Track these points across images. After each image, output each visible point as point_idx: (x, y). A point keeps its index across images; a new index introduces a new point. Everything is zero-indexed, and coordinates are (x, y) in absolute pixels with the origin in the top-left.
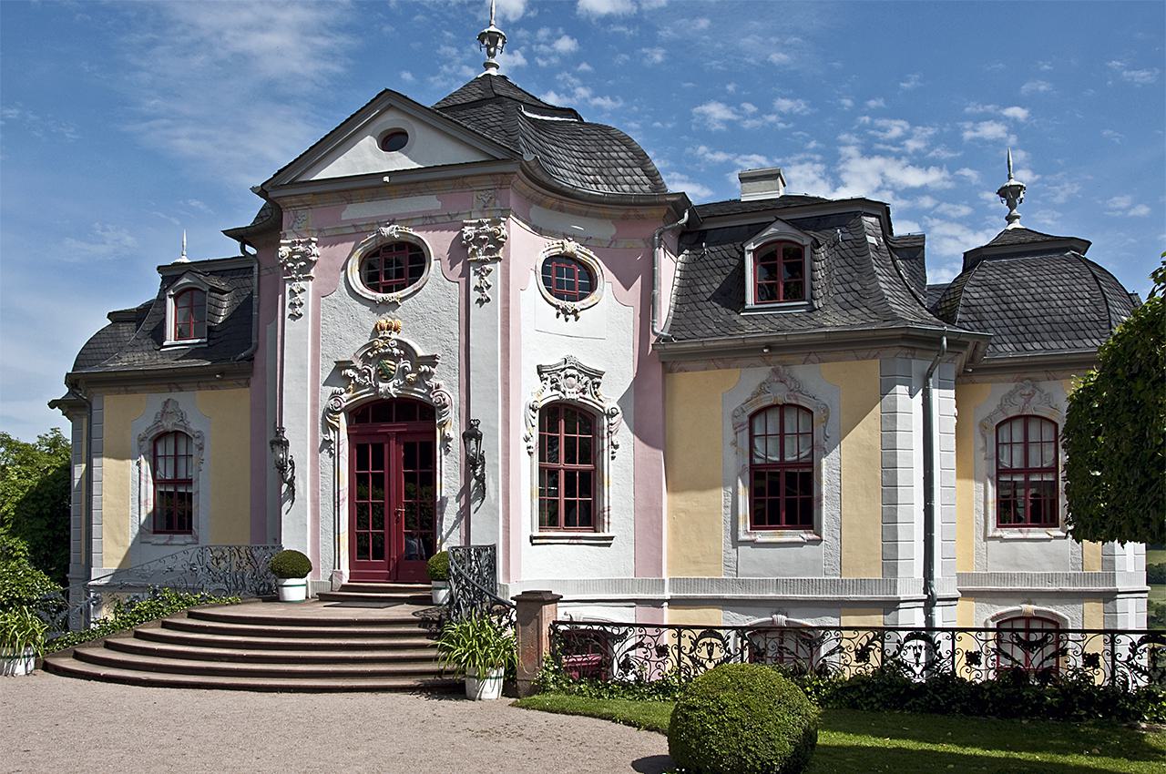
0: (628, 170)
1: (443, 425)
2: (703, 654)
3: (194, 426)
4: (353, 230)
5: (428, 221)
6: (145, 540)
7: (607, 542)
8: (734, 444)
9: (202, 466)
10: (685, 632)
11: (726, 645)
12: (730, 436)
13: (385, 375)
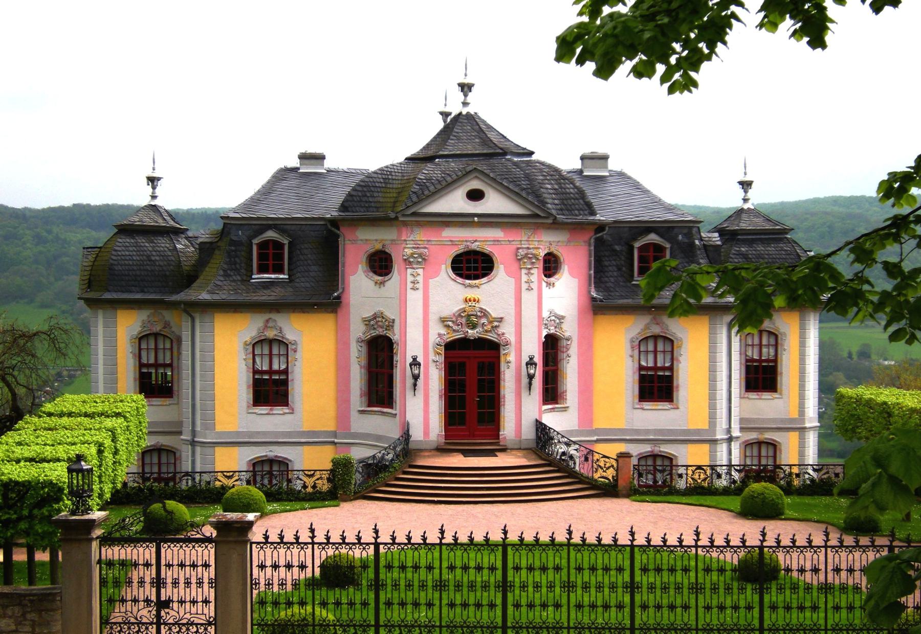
0: (577, 201)
1: (506, 355)
2: (696, 477)
3: (290, 336)
4: (450, 243)
5: (496, 243)
6: (250, 411)
7: (565, 409)
8: (632, 356)
9: (296, 363)
10: (689, 468)
11: (706, 473)
12: (630, 352)
13: (474, 326)
